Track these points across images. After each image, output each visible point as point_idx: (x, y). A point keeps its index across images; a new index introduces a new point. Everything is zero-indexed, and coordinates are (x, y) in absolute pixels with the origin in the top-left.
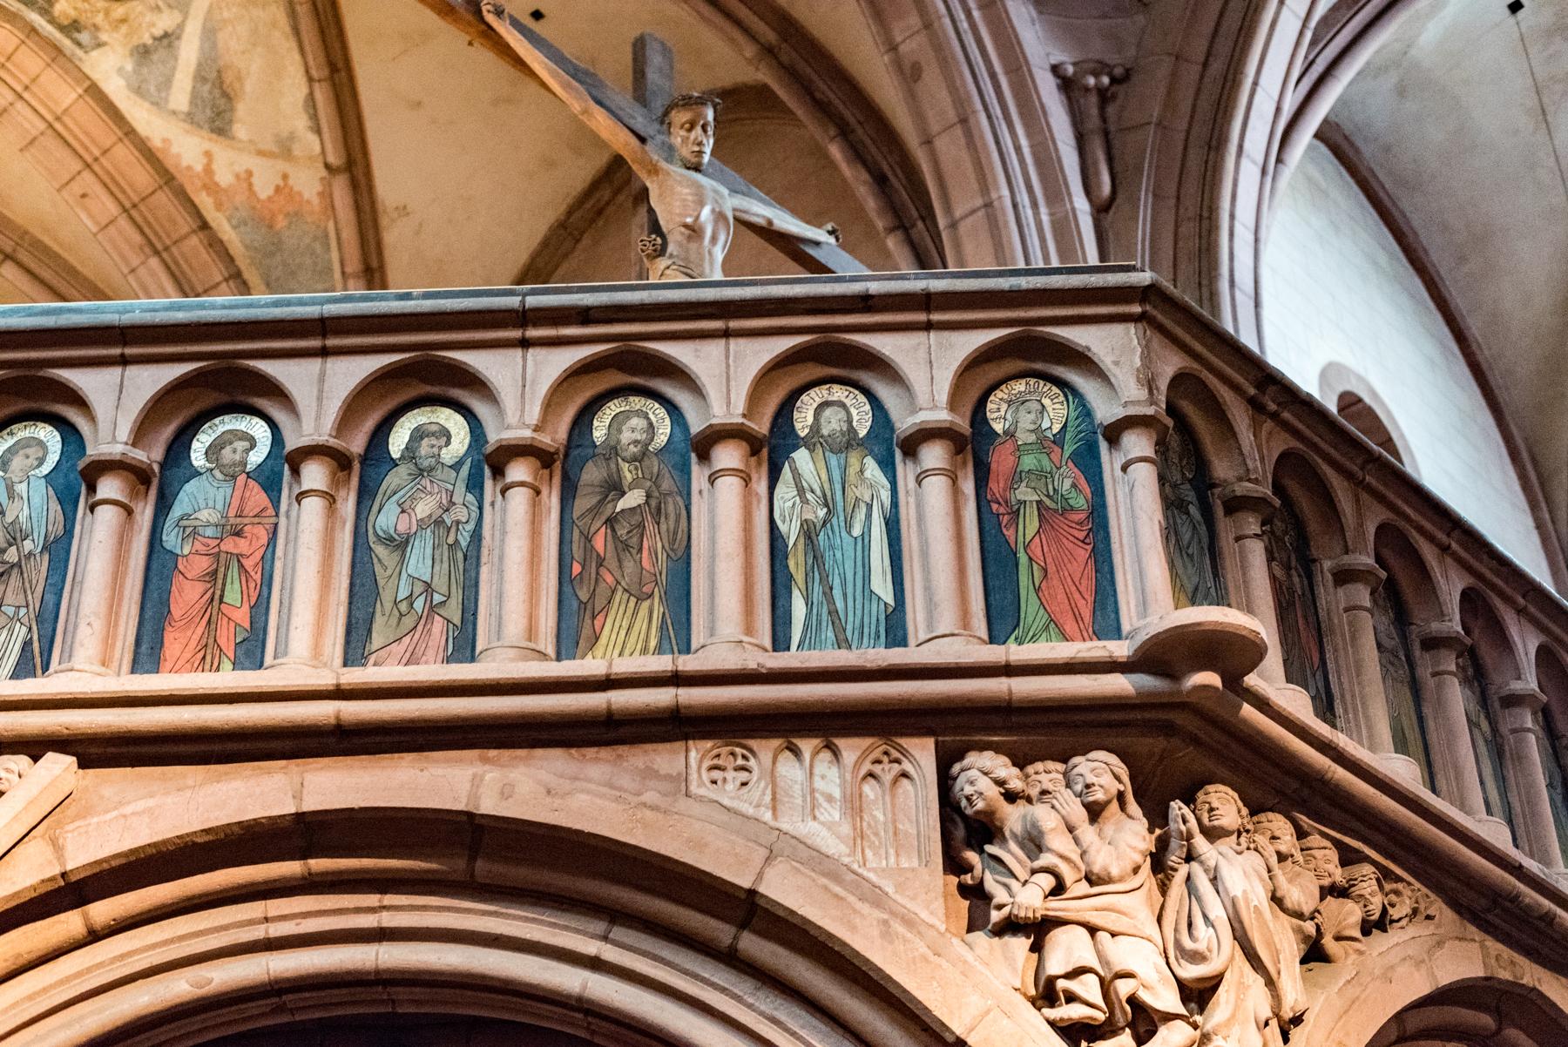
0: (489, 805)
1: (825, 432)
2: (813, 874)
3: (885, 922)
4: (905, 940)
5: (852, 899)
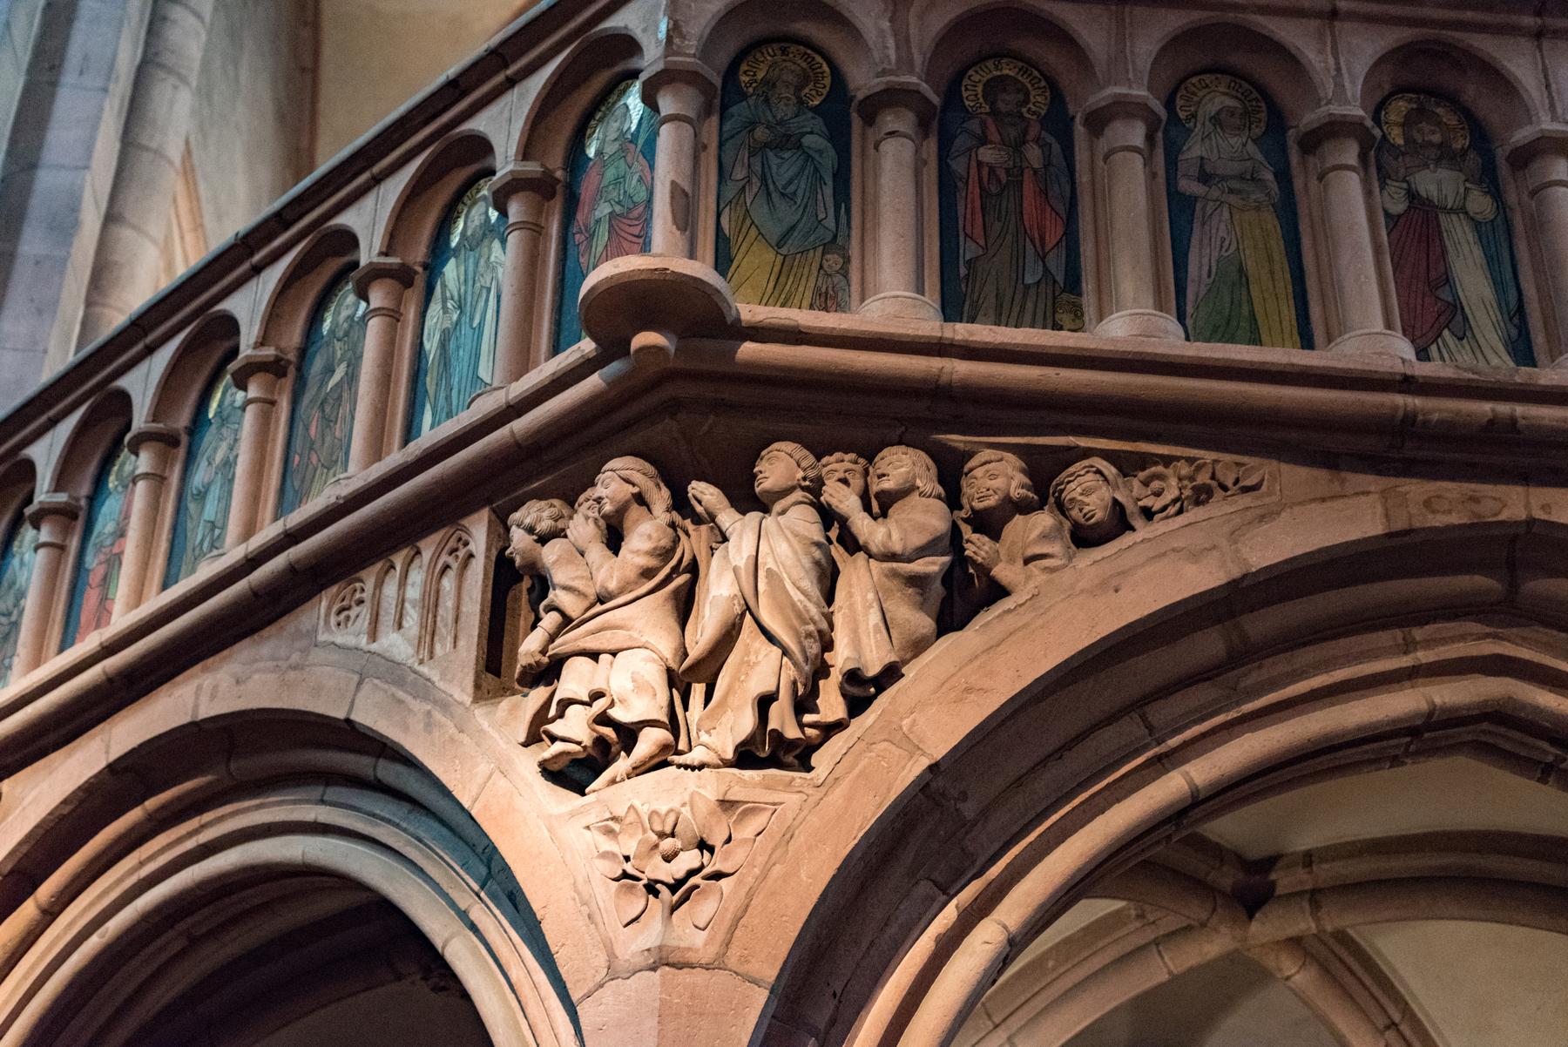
0: (207, 711)
1: (469, 233)
2: (386, 686)
3: (429, 713)
4: (441, 726)
5: (409, 699)
